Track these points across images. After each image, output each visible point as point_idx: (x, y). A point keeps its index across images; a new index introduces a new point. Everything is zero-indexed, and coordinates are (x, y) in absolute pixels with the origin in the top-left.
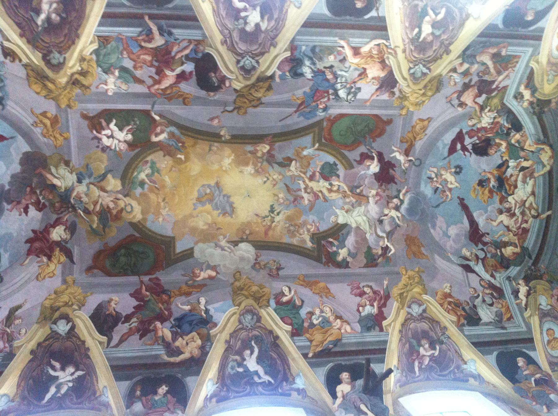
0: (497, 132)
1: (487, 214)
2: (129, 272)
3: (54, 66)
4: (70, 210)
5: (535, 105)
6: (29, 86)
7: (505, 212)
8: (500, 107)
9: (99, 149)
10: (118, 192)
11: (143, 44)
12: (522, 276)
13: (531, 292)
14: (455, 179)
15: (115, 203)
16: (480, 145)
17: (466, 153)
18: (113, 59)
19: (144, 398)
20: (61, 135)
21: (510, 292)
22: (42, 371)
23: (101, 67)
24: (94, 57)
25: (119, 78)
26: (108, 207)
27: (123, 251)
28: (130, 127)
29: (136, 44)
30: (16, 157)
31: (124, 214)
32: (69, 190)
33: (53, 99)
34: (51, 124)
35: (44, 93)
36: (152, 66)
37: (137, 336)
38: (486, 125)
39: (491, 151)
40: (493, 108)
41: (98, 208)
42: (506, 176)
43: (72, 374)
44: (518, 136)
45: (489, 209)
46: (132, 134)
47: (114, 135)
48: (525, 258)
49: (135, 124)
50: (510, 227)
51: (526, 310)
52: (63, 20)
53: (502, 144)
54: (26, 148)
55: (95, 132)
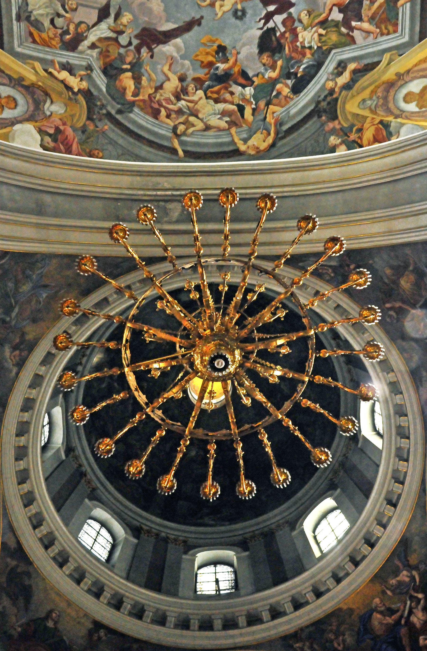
0: (292, 58)
1: (179, 58)
5: (329, 99)
7: (182, 86)
8: (324, 48)
12: (93, 90)
13: (70, 93)
14: (227, 12)
16: (274, 38)
17: (263, 21)
21: (71, 61)
38: (301, 39)
39: (265, 58)
40: (324, 39)
42: (231, 86)
44: (286, 91)
45: (187, 63)
48: (118, 103)
50: (161, 91)
51: (46, 71)
53: (274, 71)
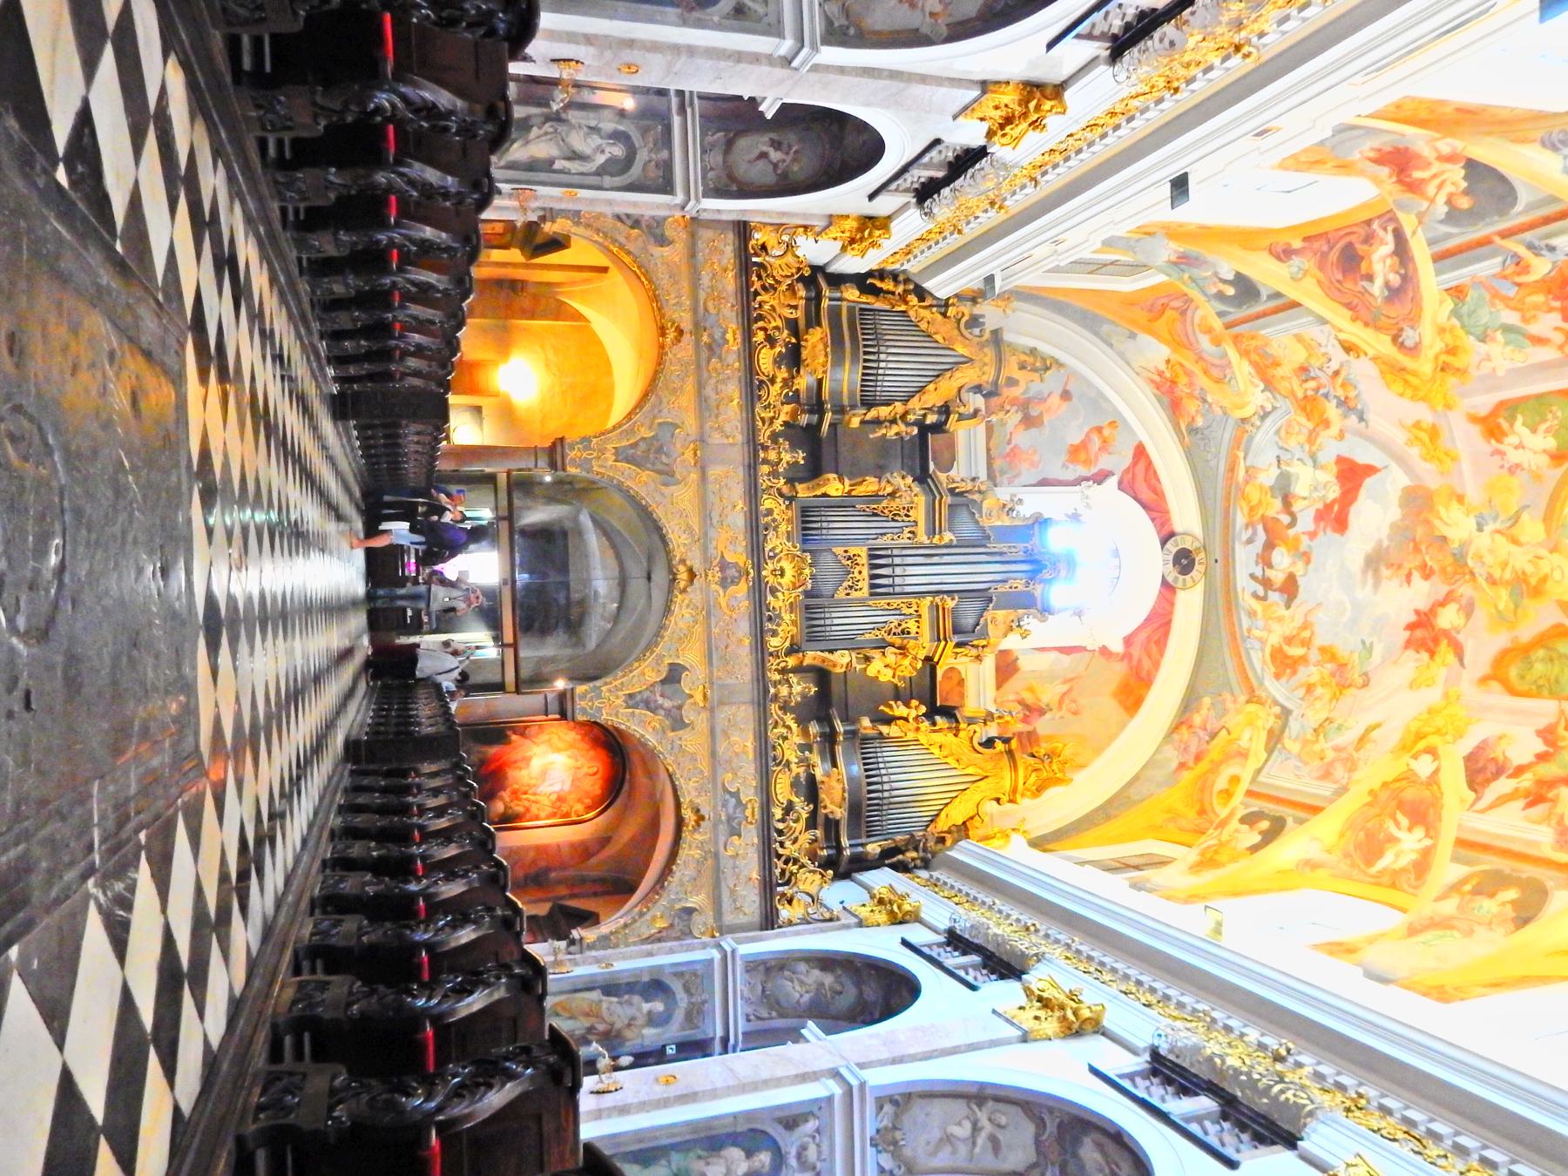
2: (1545, 692)
3: (1410, 349)
4: (1467, 577)
6: (1388, 386)
9: (1505, 471)
10: (1539, 545)
11: (1518, 279)
15: (1535, 565)
18: (1484, 316)
19: (1468, 897)
20: (1447, 454)
22: (1381, 825)
23: (1471, 334)
24: (1455, 321)
25: (1507, 343)
26: (1524, 573)
27: (1541, 653)
28: (1548, 424)
29: (1508, 284)
30: (1394, 495)
31: (1549, 585)
32: (1464, 545)
33: (1423, 399)
34: (1431, 440)
35: (1409, 392)
36: (1551, 310)
37: (1521, 803)
41: (1508, 575)
43: (1420, 841)
46: (1554, 436)
47: (1525, 444)
49: (1555, 417)
52: (1405, 278)
54: (1404, 481)
55: (1493, 441)
